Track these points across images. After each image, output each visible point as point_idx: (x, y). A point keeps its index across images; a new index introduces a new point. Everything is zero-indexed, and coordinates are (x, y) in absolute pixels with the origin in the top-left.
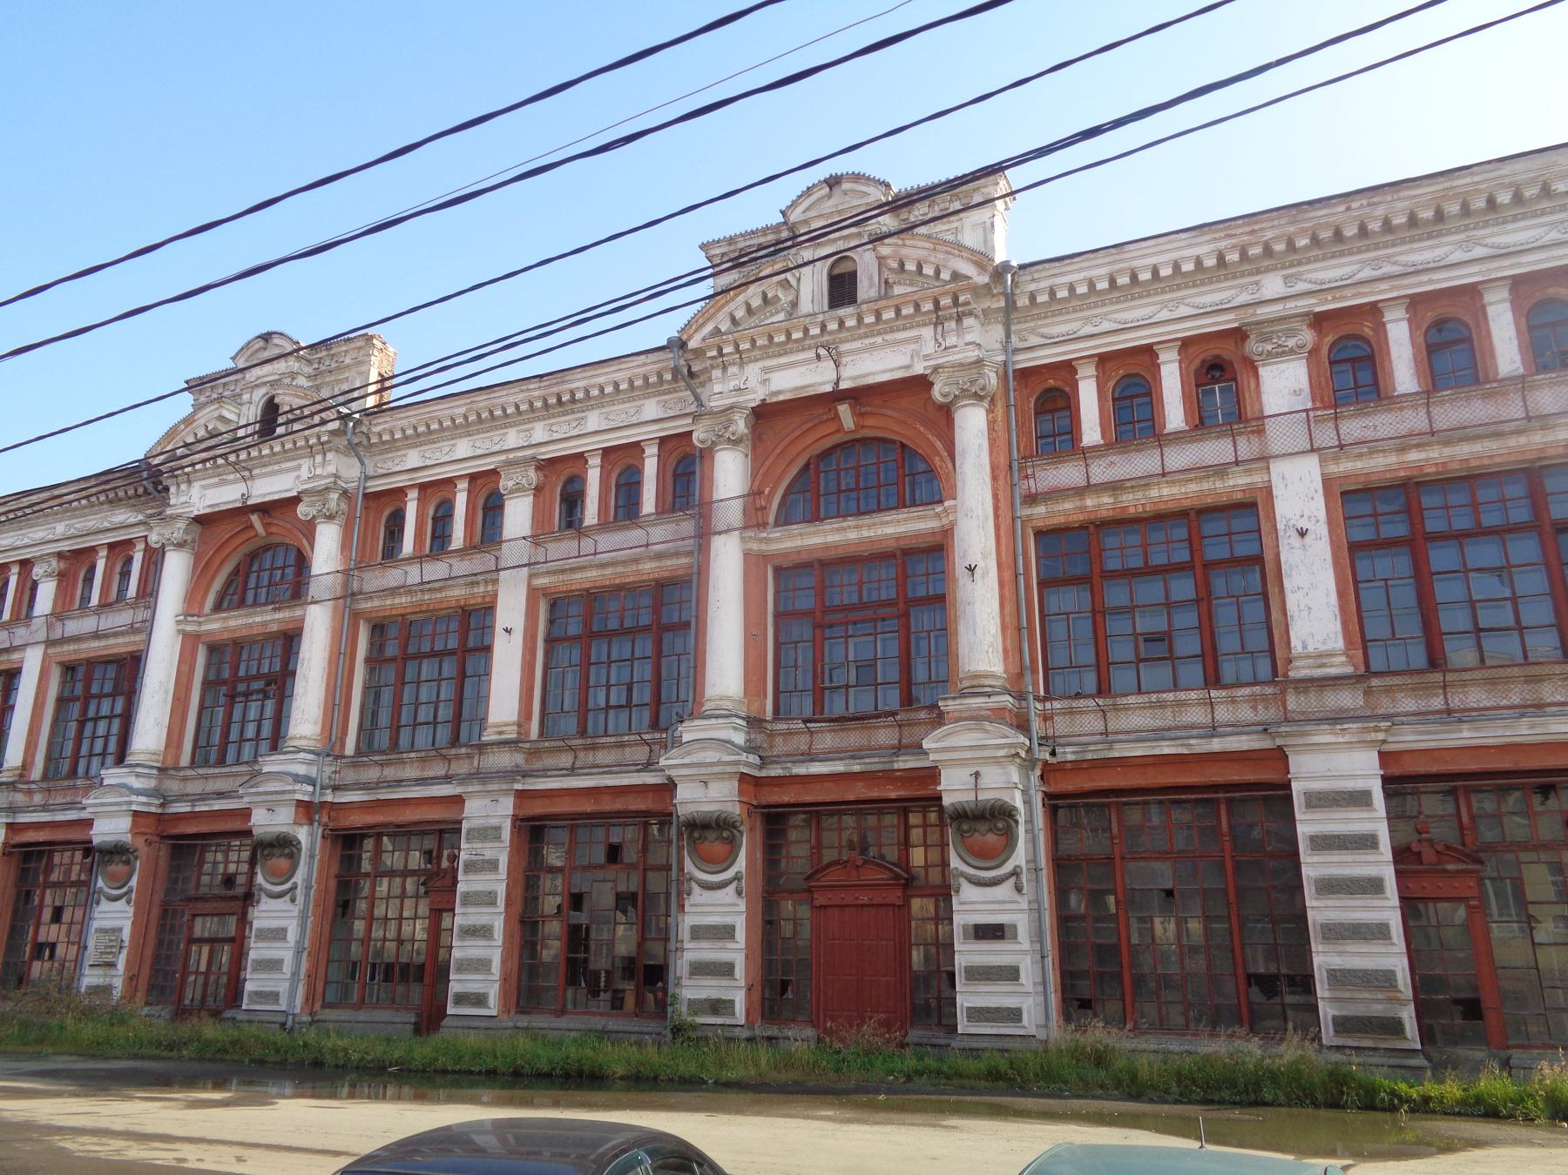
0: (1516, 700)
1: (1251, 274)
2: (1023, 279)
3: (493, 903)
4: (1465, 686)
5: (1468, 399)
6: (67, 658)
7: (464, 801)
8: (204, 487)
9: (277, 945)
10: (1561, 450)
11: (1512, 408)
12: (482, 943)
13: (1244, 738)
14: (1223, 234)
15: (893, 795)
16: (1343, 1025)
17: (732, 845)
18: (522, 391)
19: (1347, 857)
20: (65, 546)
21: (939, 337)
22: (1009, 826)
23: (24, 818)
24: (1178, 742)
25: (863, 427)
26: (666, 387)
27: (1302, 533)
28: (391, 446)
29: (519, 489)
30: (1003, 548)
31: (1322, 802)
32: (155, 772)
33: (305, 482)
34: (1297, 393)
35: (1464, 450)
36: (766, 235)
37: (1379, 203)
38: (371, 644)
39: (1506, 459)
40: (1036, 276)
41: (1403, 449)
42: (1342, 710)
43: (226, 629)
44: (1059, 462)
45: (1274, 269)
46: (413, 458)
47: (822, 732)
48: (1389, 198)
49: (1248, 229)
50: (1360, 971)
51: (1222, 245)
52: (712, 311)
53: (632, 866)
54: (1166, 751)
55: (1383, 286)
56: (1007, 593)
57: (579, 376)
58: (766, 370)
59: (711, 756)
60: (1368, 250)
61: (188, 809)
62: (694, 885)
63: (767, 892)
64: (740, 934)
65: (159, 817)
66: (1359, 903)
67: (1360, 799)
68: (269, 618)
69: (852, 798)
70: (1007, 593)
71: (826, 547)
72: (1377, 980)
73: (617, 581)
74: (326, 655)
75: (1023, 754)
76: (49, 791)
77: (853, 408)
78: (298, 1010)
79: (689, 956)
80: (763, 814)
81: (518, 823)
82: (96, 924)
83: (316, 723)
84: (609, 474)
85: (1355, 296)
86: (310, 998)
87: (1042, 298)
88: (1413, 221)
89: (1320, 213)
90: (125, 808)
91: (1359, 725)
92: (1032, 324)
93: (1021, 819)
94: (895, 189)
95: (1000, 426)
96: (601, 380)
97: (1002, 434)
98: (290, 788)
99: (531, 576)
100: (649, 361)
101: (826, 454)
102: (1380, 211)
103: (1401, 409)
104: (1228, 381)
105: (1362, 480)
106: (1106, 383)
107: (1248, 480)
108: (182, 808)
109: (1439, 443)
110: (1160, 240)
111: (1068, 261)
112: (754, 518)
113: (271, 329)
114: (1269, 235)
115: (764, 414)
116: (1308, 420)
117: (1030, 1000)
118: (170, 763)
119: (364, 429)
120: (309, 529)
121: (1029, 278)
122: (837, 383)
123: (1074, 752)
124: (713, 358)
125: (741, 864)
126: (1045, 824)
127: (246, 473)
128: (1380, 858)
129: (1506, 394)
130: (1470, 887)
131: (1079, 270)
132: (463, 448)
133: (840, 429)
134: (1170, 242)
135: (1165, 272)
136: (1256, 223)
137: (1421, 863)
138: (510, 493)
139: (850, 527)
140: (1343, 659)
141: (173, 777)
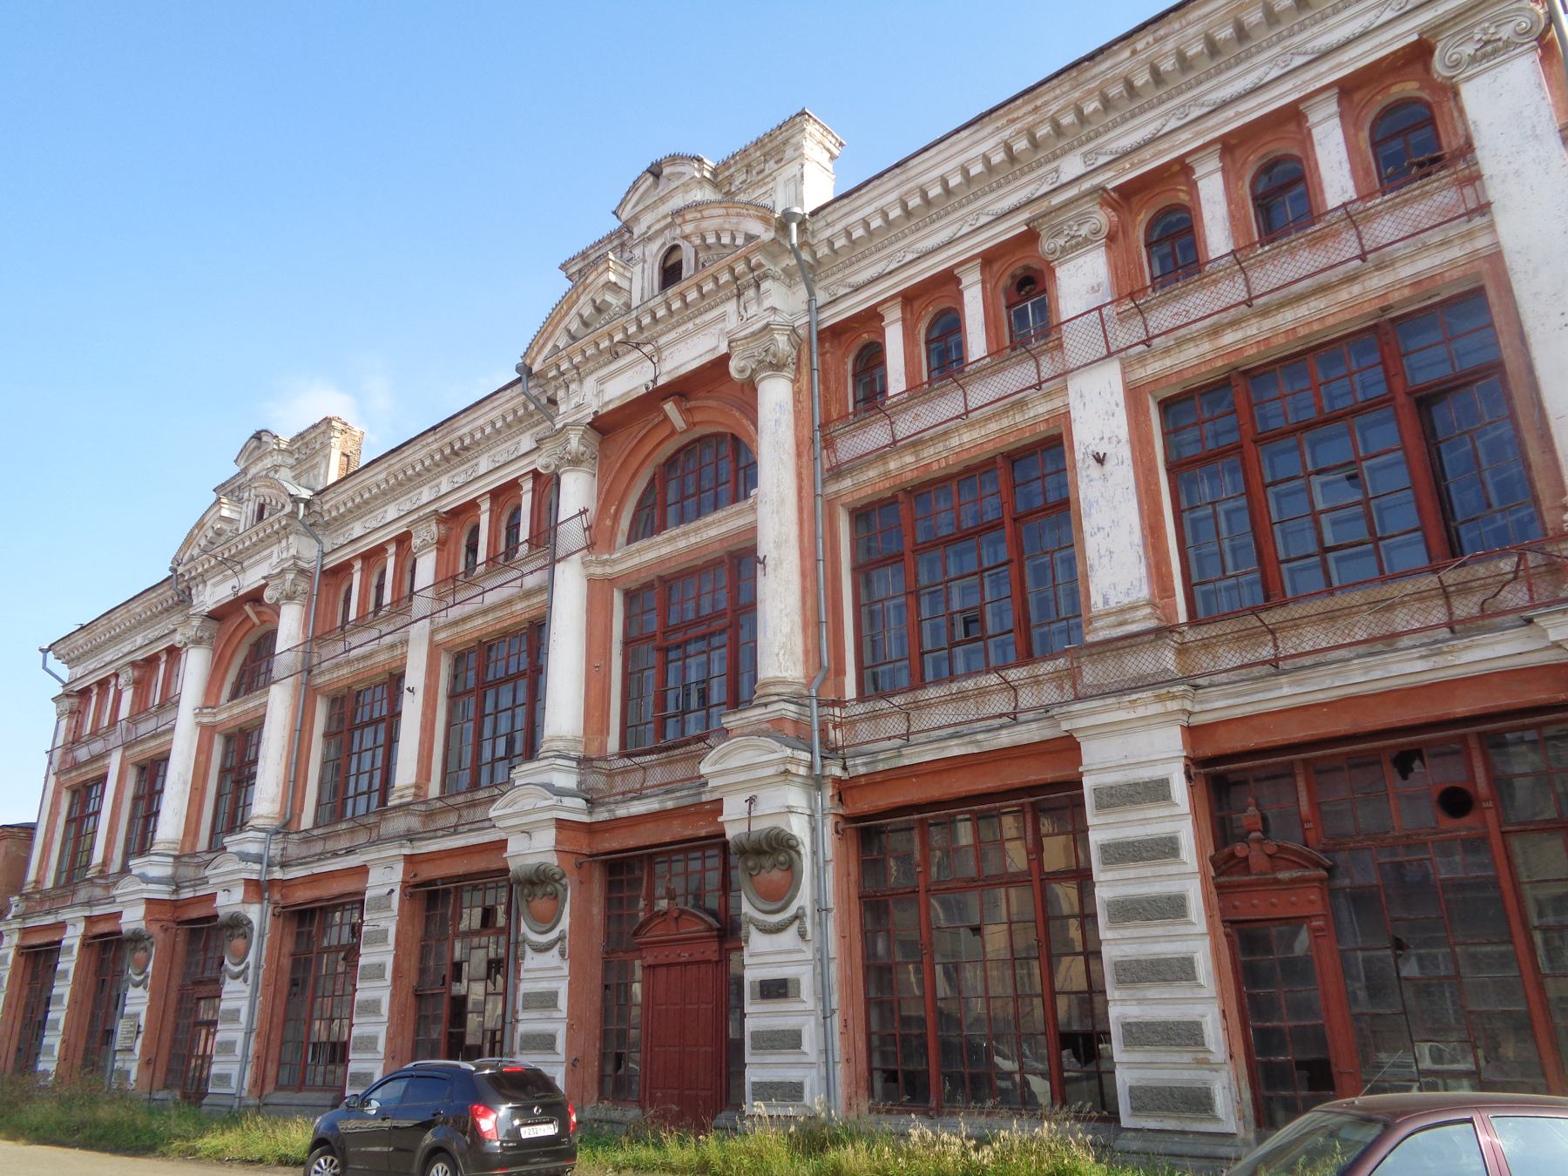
0: (1361, 635)
1: (1048, 161)
2: (817, 226)
3: (381, 977)
4: (1297, 626)
5: (1292, 252)
6: (138, 759)
7: (367, 872)
8: (214, 585)
10: (1407, 292)
11: (1348, 246)
12: (373, 1019)
13: (1034, 726)
14: (1004, 121)
15: (703, 833)
17: (557, 898)
18: (424, 446)
19: (1145, 870)
20: (139, 656)
21: (742, 309)
22: (791, 860)
23: (97, 911)
24: (967, 739)
25: (695, 424)
26: (536, 418)
27: (1100, 460)
28: (340, 521)
29: (425, 546)
30: (806, 533)
31: (1114, 800)
32: (171, 860)
33: (275, 567)
34: (1094, 290)
35: (1287, 318)
36: (611, 242)
37: (1167, 35)
38: (330, 718)
39: (1340, 317)
40: (830, 219)
41: (1215, 331)
42: (1141, 677)
43: (232, 718)
44: (869, 424)
45: (1072, 148)
46: (357, 530)
47: (652, 766)
48: (1177, 26)
49: (1030, 107)
50: (1160, 1024)
51: (1006, 134)
52: (550, 329)
53: (501, 931)
54: (956, 752)
55: (1185, 135)
56: (809, 585)
57: (464, 421)
58: (601, 381)
59: (527, 804)
60: (1170, 98)
61: (191, 895)
62: (527, 948)
63: (607, 953)
64: (563, 1002)
65: (175, 905)
66: (1159, 931)
67: (1157, 791)
69: (667, 839)
70: (809, 585)
71: (662, 561)
72: (1179, 1034)
73: (498, 627)
74: (286, 733)
75: (802, 771)
77: (676, 403)
78: (244, 1094)
79: (522, 1028)
80: (605, 861)
81: (410, 890)
83: (273, 801)
84: (498, 519)
85: (1155, 156)
86: (260, 1082)
87: (840, 243)
88: (1213, 48)
89: (1104, 67)
90: (139, 896)
91: (1149, 693)
92: (840, 275)
93: (806, 850)
94: (710, 163)
95: (804, 397)
96: (481, 422)
97: (806, 403)
98: (236, 867)
99: (433, 632)
100: (514, 394)
101: (671, 462)
102: (1170, 45)
103: (1215, 282)
104: (1039, 294)
105: (1174, 380)
106: (915, 325)
107: (1049, 406)
108: (187, 894)
109: (1256, 315)
110: (942, 146)
111: (856, 195)
112: (597, 539)
113: (259, 429)
114: (1054, 107)
115: (605, 426)
116: (1102, 320)
117: (814, 1072)
118: (187, 850)
119: (317, 508)
120: (276, 609)
121: (823, 223)
122: (654, 381)
123: (865, 764)
124: (554, 378)
125: (565, 923)
126: (837, 853)
127: (238, 568)
128: (1183, 869)
129: (1336, 234)
130: (1312, 902)
131: (869, 203)
132: (392, 512)
133: (673, 432)
134: (952, 145)
135: (954, 181)
136: (1037, 98)
137: (1247, 870)
138: (419, 551)
139: (678, 535)
140: (1148, 610)
141: (187, 864)
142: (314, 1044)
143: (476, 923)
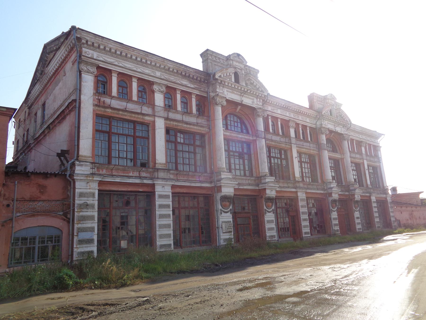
8: (227, 91)
9: (271, 224)
16: (377, 227)
51: (361, 130)
58: (328, 123)
61: (237, 187)
68: (243, 137)
73: (307, 152)
76: (177, 174)
82: (221, 220)
125: (336, 208)
142: (280, 228)
143: (311, 206)
